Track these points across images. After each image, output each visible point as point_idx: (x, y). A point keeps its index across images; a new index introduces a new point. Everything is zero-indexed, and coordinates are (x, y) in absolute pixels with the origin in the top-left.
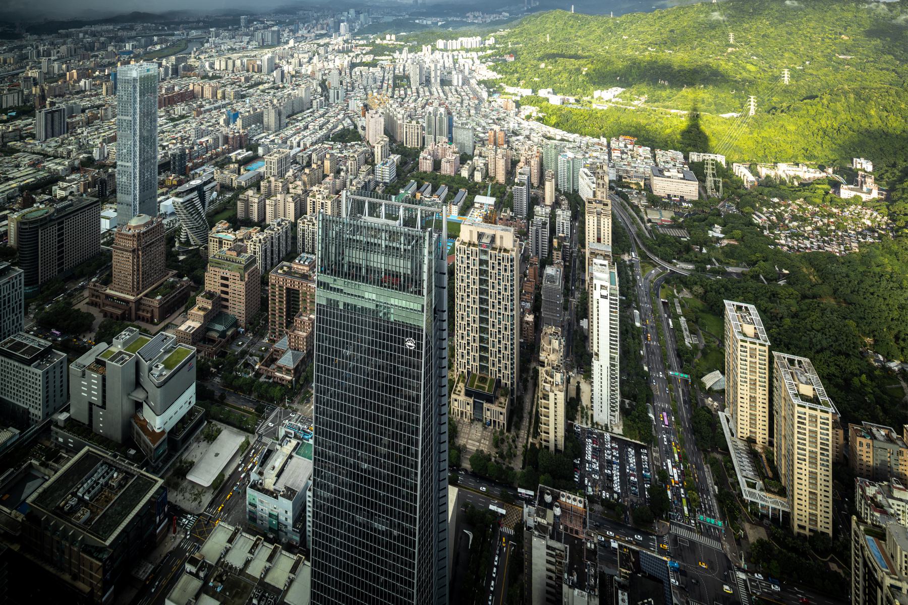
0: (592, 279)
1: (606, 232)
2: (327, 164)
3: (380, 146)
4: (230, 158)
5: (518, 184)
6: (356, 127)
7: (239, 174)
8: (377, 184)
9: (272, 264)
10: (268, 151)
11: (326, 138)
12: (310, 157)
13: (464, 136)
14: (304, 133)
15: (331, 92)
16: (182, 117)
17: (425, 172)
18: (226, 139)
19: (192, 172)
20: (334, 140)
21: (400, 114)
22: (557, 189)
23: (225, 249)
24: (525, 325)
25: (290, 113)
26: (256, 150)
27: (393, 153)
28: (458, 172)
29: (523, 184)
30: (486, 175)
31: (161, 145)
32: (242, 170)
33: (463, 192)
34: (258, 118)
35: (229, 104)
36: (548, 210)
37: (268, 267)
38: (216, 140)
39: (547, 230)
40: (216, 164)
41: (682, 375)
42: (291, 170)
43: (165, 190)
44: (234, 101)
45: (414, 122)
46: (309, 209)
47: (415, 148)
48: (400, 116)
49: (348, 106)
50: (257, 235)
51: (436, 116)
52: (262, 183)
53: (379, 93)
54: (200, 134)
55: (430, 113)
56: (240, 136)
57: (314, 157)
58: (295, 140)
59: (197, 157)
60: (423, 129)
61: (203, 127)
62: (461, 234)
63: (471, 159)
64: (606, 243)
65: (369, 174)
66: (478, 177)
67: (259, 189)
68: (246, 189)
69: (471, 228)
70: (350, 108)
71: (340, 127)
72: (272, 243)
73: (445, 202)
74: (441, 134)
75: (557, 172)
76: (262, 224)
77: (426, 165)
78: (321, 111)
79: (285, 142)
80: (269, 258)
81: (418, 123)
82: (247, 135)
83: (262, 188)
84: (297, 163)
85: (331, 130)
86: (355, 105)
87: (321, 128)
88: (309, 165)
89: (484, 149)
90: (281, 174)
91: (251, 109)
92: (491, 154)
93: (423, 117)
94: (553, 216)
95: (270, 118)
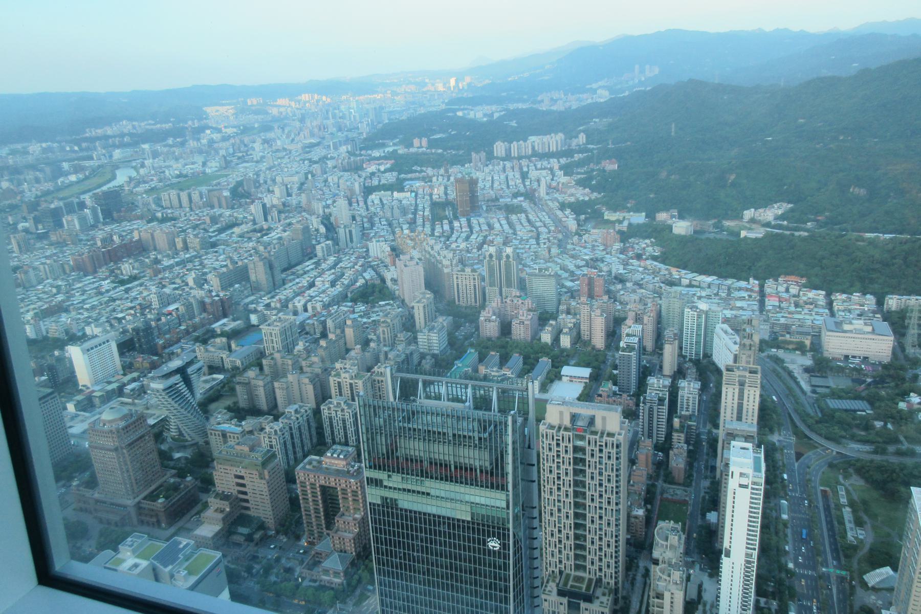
0: (727, 465)
1: (751, 407)
2: (349, 332)
3: (421, 305)
4: (213, 331)
5: (624, 350)
6: (383, 280)
7: (230, 349)
8: (423, 356)
9: (296, 458)
10: (264, 319)
11: (342, 298)
12: (324, 323)
13: (545, 288)
14: (312, 292)
15: (341, 231)
16: (134, 278)
17: (489, 339)
18: (203, 305)
19: (167, 351)
20: (354, 301)
21: (446, 259)
22: (680, 355)
23: (231, 442)
24: (633, 520)
27: (442, 314)
28: (536, 337)
30: (578, 339)
31: (116, 318)
32: (233, 346)
33: (545, 362)
34: (241, 275)
35: (196, 257)
36: (668, 382)
37: (292, 463)
38: (189, 306)
39: (665, 408)
40: (197, 340)
41: (838, 572)
42: (301, 343)
43: (135, 375)
44: (202, 252)
45: (468, 270)
46: (333, 391)
47: (471, 307)
49: (368, 251)
50: (272, 427)
51: (500, 259)
52: (264, 362)
53: (412, 231)
54: (166, 301)
55: (491, 256)
56: (222, 301)
57: (330, 324)
58: (299, 303)
59: (169, 331)
60: (483, 279)
61: (167, 290)
62: (547, 415)
63: (555, 319)
64: (749, 421)
65: (409, 344)
66: (566, 341)
67: (261, 369)
68: (245, 369)
69: (562, 408)
70: (371, 253)
71: (360, 282)
72: (292, 434)
73: (521, 375)
74: (509, 285)
75: (681, 331)
76: (274, 412)
78: (332, 260)
79: (285, 305)
80: (290, 452)
81: (474, 271)
82: (231, 298)
83: (266, 368)
84: (307, 333)
85: (348, 286)
86: (378, 249)
88: (324, 335)
89: (574, 304)
90: (288, 349)
91: (228, 262)
92: (584, 311)
93: (480, 262)
94: (674, 392)
95: (259, 274)
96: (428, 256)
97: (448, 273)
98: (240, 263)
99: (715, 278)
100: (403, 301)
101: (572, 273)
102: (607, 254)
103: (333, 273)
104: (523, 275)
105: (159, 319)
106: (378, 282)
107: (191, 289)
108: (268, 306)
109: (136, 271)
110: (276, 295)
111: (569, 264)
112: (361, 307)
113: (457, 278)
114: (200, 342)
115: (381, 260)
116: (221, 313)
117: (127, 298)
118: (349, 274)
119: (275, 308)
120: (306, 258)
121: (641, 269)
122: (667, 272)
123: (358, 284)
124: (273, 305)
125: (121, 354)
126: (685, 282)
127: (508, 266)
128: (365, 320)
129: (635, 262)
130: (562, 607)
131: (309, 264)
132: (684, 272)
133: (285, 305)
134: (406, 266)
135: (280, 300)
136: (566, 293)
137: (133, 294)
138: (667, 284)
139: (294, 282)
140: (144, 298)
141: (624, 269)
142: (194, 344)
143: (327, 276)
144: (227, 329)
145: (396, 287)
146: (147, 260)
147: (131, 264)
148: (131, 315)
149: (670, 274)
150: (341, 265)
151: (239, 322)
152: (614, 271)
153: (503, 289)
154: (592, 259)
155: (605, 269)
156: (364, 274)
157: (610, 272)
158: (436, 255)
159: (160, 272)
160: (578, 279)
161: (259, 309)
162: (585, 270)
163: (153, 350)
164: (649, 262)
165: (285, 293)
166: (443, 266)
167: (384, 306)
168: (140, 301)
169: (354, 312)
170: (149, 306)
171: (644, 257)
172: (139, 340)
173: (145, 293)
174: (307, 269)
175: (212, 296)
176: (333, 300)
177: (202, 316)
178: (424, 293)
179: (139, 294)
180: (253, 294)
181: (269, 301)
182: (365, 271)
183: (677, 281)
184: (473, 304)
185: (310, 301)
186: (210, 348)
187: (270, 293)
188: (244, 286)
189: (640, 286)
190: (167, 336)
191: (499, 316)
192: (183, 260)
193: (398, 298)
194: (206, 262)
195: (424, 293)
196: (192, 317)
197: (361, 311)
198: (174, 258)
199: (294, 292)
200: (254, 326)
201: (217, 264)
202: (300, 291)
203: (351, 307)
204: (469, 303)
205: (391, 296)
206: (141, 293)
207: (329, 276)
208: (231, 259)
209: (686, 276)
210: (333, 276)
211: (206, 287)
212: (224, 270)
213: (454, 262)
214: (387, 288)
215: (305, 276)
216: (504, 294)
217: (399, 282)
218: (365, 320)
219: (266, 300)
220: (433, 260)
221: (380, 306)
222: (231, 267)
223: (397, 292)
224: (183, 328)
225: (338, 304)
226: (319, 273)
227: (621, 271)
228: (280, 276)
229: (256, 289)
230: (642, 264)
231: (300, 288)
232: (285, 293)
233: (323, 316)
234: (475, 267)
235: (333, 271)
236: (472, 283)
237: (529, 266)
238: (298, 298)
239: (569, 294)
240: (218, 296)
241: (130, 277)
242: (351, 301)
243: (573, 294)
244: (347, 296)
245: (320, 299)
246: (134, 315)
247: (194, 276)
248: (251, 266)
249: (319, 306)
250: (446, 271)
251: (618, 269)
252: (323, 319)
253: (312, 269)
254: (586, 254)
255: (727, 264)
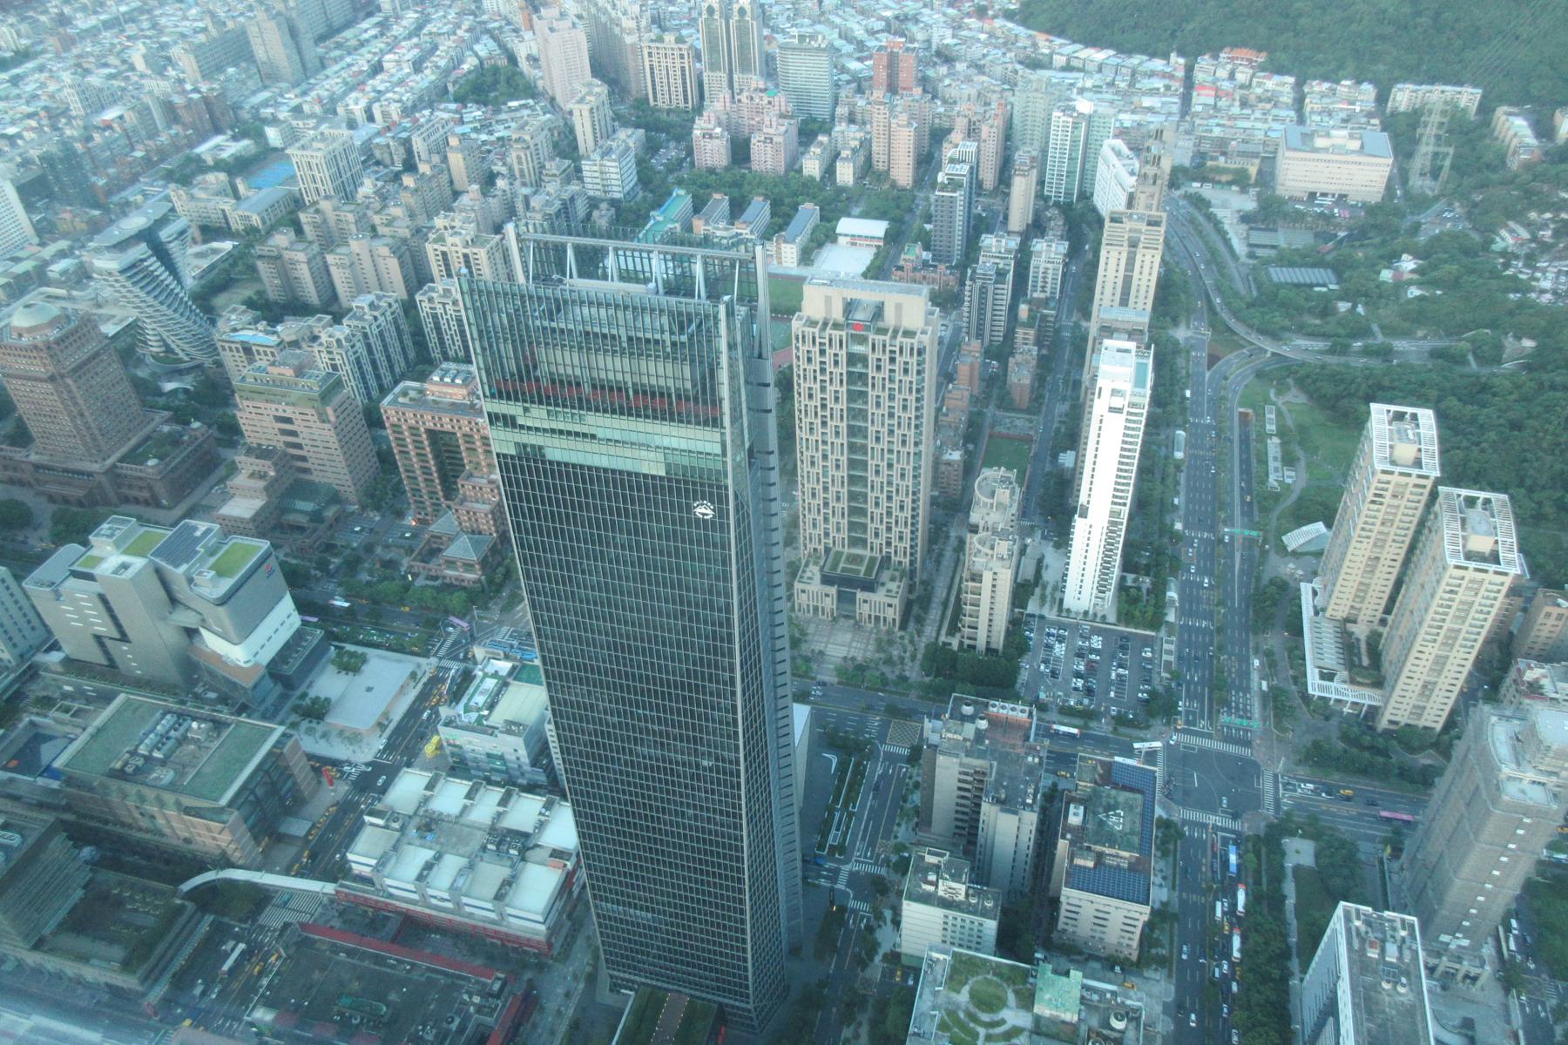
2: (456, 161)
3: (585, 108)
6: (512, 59)
8: (593, 203)
10: (292, 136)
11: (438, 94)
12: (407, 144)
14: (378, 82)
17: (711, 171)
18: (171, 112)
19: (115, 199)
20: (461, 99)
22: (1040, 196)
23: (262, 362)
25: (322, 29)
26: (259, 136)
27: (625, 124)
28: (794, 166)
29: (960, 186)
30: (867, 168)
32: (241, 188)
33: (809, 211)
34: (236, 48)
37: (375, 393)
38: (144, 112)
40: (169, 177)
43: (63, 244)
45: (669, 38)
46: (436, 268)
47: (677, 111)
48: (628, 23)
50: (331, 333)
56: (206, 100)
57: (418, 145)
58: (356, 104)
60: (698, 57)
61: (95, 80)
63: (828, 132)
66: (845, 174)
68: (270, 231)
71: (469, 64)
72: (369, 346)
74: (745, 66)
75: (1044, 152)
76: (333, 309)
77: (712, 151)
78: (411, 16)
79: (330, 109)
81: (680, 40)
82: (222, 95)
84: (378, 163)
85: (446, 72)
87: (418, 66)
88: (410, 166)
89: (861, 103)
90: (346, 193)
91: (207, 22)
92: (879, 116)
93: (692, 22)
95: (270, 45)
96: (593, 10)
97: (633, 45)
98: (230, 25)
99: (1111, 52)
100: (553, 100)
101: (861, 45)
102: (925, 6)
103: (416, 46)
104: (773, 49)
105: (89, 139)
106: (503, 62)
107: (142, 76)
108: (297, 110)
109: (24, 42)
110: (311, 89)
111: (856, 27)
112: (474, 113)
113: (650, 55)
114: (176, 181)
115: (506, 18)
116: (208, 126)
117: (19, 97)
118: (446, 46)
119: (313, 115)
120: (362, 14)
121: (983, 37)
122: (1028, 43)
123: (466, 67)
124: (306, 108)
125: (29, 207)
126: (1059, 60)
127: (743, 31)
128: (484, 137)
129: (972, 22)
130: (891, 610)
131: (368, 27)
132: (1058, 41)
133: (330, 109)
134: (552, 30)
135: (320, 100)
136: (848, 82)
137: (30, 88)
138: (1028, 66)
139: (343, 64)
140: (52, 96)
141: (954, 36)
142: (165, 187)
143: (403, 51)
144: (225, 155)
145: (537, 73)
146: (43, 18)
147: (12, 25)
148: (32, 129)
149: (1035, 45)
150: (429, 28)
151: (246, 142)
152: (935, 41)
153: (735, 77)
154: (897, 18)
155: (920, 36)
156: (477, 47)
157: (928, 41)
158: (609, 8)
159: (73, 42)
160: (870, 57)
161: (281, 116)
162: (884, 39)
163: (92, 199)
164: (999, 23)
165: (327, 84)
166: (622, 30)
167: (516, 109)
168: (44, 101)
169: (461, 122)
170: (65, 112)
171: (990, 13)
172: (57, 178)
173: (52, 87)
174: (365, 36)
175: (184, 92)
176: (421, 99)
177: (173, 132)
178: (589, 85)
179: (40, 88)
180: (265, 87)
181: (298, 101)
182: (477, 40)
183: (1046, 59)
184: (682, 105)
185: (378, 100)
186: (197, 192)
187: (296, 84)
188: (246, 70)
189: (980, 69)
190: (111, 171)
191: (728, 128)
192: (117, 18)
193: (542, 94)
194: (163, 21)
195: (589, 85)
196: (153, 134)
197: (475, 120)
198: (96, 12)
199: (345, 83)
200: (275, 150)
201: (185, 27)
202: (355, 81)
203: (456, 112)
204: (674, 103)
205: (530, 91)
206: (43, 85)
207: (408, 52)
208: (213, 15)
209: (1062, 49)
210: (416, 52)
211: (171, 72)
212: (201, 38)
213: (643, 23)
214: (521, 73)
215: (363, 50)
216: (736, 86)
217: (543, 62)
218: (484, 137)
219: (292, 98)
220: (603, 19)
221: (511, 110)
222: (214, 32)
223: (540, 84)
224: (139, 154)
225: (431, 105)
226: (388, 44)
227: (949, 41)
228: (314, 52)
229: (268, 77)
230: (987, 27)
231: (355, 75)
232: (329, 84)
233: (405, 130)
234: (684, 32)
235: (415, 40)
236: (678, 65)
237: (783, 31)
238: (354, 95)
239: (854, 85)
240: (196, 90)
241: (17, 52)
242: (456, 101)
243: (860, 85)
244: (446, 91)
245: (396, 97)
246: (39, 130)
247: (143, 50)
248: (253, 31)
249: (394, 109)
250: (629, 40)
251: (943, 37)
252: (404, 135)
253: (375, 37)
254: (887, 7)
255: (1136, 26)
